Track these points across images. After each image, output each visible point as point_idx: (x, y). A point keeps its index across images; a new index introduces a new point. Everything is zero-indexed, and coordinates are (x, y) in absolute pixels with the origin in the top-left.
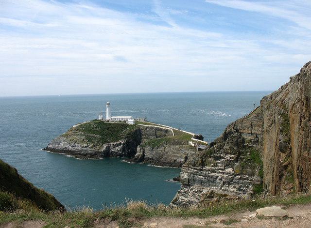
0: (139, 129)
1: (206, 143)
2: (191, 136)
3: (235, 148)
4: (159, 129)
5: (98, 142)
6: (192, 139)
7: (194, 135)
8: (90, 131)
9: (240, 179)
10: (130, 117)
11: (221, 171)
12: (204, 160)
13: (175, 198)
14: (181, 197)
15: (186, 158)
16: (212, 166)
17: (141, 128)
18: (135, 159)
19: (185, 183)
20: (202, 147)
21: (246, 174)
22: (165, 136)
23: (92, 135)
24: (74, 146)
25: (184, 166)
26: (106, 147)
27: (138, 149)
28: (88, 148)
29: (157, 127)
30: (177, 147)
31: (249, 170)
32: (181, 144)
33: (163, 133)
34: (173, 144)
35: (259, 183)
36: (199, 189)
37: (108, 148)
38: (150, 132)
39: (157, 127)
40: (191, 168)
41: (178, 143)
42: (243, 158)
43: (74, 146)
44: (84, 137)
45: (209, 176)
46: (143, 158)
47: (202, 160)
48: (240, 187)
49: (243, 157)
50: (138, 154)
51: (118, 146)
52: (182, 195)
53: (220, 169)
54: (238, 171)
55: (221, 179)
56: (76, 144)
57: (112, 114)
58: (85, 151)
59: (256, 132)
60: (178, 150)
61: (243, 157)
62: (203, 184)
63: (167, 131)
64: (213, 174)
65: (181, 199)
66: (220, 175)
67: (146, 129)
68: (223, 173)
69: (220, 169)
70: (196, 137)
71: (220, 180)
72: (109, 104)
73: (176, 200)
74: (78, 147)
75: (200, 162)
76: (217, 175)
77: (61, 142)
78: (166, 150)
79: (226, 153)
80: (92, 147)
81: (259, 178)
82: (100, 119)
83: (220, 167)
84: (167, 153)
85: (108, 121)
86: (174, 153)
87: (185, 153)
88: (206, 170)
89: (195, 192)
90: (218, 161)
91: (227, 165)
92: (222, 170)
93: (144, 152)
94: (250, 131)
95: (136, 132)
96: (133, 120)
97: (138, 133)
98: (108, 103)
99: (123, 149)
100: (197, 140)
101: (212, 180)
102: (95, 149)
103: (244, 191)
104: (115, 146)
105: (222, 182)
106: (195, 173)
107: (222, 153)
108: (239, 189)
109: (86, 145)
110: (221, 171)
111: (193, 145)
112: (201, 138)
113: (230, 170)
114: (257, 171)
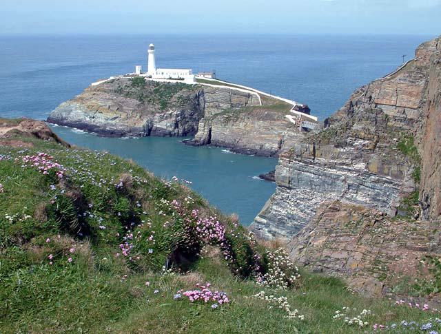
0: (203, 92)
1: (315, 119)
2: (289, 106)
3: (373, 129)
4: (235, 93)
5: (133, 111)
6: (291, 111)
7: (295, 105)
8: (119, 91)
9: (377, 181)
10: (187, 71)
11: (345, 167)
12: (317, 147)
13: (264, 209)
14: (275, 207)
15: (280, 143)
16: (332, 158)
18: (196, 141)
19: (283, 184)
20: (308, 125)
21: (388, 175)
22: (246, 103)
23: (121, 98)
24: (94, 117)
25: (282, 156)
26: (147, 121)
27: (201, 124)
28: (117, 120)
29: (234, 88)
30: (267, 123)
31: (394, 168)
32: (275, 120)
33: (244, 99)
34: (259, 119)
35: (411, 190)
36: (306, 196)
38: (219, 96)
39: (234, 88)
40: (296, 160)
42: (386, 147)
43: (94, 117)
44: (110, 103)
45: (325, 175)
46: (209, 141)
47: (314, 148)
48: (378, 195)
49: (384, 145)
50: (201, 134)
51: (167, 118)
52: (277, 204)
53: (344, 164)
54: (373, 168)
55: (344, 181)
56: (98, 114)
57: (160, 63)
58: (113, 126)
59: (404, 104)
60: (266, 128)
61: (384, 145)
62: (313, 187)
63: (249, 96)
64: (334, 171)
65: (276, 211)
67: (213, 91)
68: (350, 170)
69: (344, 164)
70: (300, 109)
71: (344, 180)
72: (152, 48)
73: (268, 211)
74: (100, 120)
75: (312, 150)
76: (339, 173)
77: (71, 111)
78: (248, 129)
79: (357, 137)
80: (124, 120)
81: (411, 182)
82: (138, 72)
84: (248, 132)
85: (150, 77)
86: (261, 133)
87: (279, 135)
88: (320, 165)
89: (300, 199)
91: (356, 157)
92: (347, 165)
93: (210, 131)
94: (393, 103)
95: (197, 97)
96: (193, 76)
98: (151, 45)
99: (176, 126)
100: (300, 113)
101: (330, 182)
102: (130, 123)
103: (384, 201)
104: (162, 119)
105: (346, 185)
106: (301, 169)
107: (348, 137)
108: (374, 199)
109: (115, 116)
110: (345, 167)
111: (294, 122)
112: (307, 110)
113: (362, 166)
114: (408, 171)
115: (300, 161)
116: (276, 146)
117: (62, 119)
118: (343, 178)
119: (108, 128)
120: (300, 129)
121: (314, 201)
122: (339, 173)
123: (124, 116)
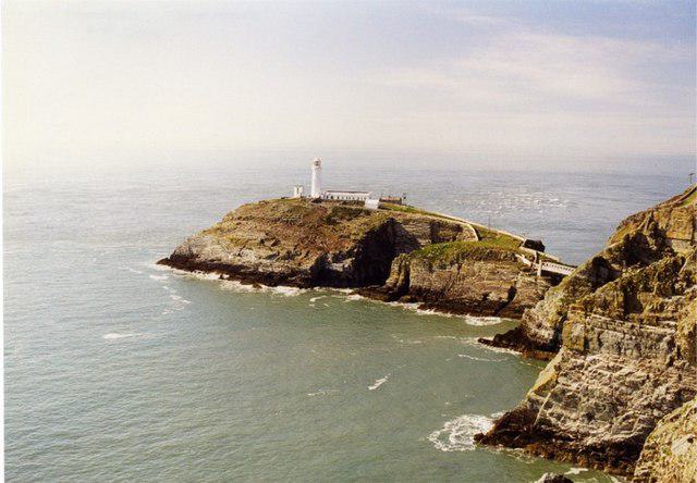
7: (524, 240)
17: (399, 219)
22: (454, 239)
25: (574, 308)
30: (490, 266)
32: (499, 260)
33: (451, 233)
37: (322, 261)
40: (595, 313)
41: (491, 256)
44: (262, 236)
56: (246, 251)
58: (267, 266)
62: (622, 351)
66: (668, 331)
67: (407, 222)
75: (621, 299)
76: (660, 330)
80: (284, 258)
83: (670, 315)
90: (667, 300)
95: (384, 227)
97: (389, 229)
115: (603, 315)
116: (505, 296)
117: (193, 256)
118: (668, 338)
119: (260, 270)
120: (539, 273)
121: (625, 370)
122: (660, 330)
123: (283, 253)
